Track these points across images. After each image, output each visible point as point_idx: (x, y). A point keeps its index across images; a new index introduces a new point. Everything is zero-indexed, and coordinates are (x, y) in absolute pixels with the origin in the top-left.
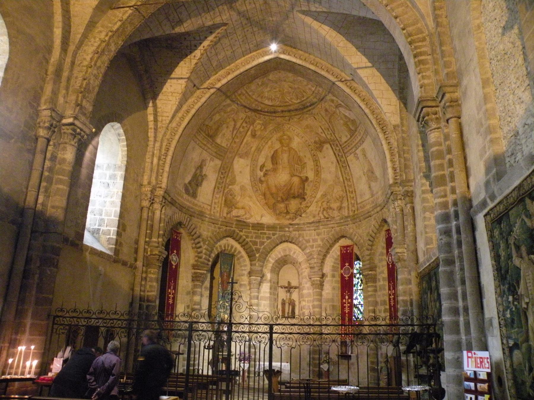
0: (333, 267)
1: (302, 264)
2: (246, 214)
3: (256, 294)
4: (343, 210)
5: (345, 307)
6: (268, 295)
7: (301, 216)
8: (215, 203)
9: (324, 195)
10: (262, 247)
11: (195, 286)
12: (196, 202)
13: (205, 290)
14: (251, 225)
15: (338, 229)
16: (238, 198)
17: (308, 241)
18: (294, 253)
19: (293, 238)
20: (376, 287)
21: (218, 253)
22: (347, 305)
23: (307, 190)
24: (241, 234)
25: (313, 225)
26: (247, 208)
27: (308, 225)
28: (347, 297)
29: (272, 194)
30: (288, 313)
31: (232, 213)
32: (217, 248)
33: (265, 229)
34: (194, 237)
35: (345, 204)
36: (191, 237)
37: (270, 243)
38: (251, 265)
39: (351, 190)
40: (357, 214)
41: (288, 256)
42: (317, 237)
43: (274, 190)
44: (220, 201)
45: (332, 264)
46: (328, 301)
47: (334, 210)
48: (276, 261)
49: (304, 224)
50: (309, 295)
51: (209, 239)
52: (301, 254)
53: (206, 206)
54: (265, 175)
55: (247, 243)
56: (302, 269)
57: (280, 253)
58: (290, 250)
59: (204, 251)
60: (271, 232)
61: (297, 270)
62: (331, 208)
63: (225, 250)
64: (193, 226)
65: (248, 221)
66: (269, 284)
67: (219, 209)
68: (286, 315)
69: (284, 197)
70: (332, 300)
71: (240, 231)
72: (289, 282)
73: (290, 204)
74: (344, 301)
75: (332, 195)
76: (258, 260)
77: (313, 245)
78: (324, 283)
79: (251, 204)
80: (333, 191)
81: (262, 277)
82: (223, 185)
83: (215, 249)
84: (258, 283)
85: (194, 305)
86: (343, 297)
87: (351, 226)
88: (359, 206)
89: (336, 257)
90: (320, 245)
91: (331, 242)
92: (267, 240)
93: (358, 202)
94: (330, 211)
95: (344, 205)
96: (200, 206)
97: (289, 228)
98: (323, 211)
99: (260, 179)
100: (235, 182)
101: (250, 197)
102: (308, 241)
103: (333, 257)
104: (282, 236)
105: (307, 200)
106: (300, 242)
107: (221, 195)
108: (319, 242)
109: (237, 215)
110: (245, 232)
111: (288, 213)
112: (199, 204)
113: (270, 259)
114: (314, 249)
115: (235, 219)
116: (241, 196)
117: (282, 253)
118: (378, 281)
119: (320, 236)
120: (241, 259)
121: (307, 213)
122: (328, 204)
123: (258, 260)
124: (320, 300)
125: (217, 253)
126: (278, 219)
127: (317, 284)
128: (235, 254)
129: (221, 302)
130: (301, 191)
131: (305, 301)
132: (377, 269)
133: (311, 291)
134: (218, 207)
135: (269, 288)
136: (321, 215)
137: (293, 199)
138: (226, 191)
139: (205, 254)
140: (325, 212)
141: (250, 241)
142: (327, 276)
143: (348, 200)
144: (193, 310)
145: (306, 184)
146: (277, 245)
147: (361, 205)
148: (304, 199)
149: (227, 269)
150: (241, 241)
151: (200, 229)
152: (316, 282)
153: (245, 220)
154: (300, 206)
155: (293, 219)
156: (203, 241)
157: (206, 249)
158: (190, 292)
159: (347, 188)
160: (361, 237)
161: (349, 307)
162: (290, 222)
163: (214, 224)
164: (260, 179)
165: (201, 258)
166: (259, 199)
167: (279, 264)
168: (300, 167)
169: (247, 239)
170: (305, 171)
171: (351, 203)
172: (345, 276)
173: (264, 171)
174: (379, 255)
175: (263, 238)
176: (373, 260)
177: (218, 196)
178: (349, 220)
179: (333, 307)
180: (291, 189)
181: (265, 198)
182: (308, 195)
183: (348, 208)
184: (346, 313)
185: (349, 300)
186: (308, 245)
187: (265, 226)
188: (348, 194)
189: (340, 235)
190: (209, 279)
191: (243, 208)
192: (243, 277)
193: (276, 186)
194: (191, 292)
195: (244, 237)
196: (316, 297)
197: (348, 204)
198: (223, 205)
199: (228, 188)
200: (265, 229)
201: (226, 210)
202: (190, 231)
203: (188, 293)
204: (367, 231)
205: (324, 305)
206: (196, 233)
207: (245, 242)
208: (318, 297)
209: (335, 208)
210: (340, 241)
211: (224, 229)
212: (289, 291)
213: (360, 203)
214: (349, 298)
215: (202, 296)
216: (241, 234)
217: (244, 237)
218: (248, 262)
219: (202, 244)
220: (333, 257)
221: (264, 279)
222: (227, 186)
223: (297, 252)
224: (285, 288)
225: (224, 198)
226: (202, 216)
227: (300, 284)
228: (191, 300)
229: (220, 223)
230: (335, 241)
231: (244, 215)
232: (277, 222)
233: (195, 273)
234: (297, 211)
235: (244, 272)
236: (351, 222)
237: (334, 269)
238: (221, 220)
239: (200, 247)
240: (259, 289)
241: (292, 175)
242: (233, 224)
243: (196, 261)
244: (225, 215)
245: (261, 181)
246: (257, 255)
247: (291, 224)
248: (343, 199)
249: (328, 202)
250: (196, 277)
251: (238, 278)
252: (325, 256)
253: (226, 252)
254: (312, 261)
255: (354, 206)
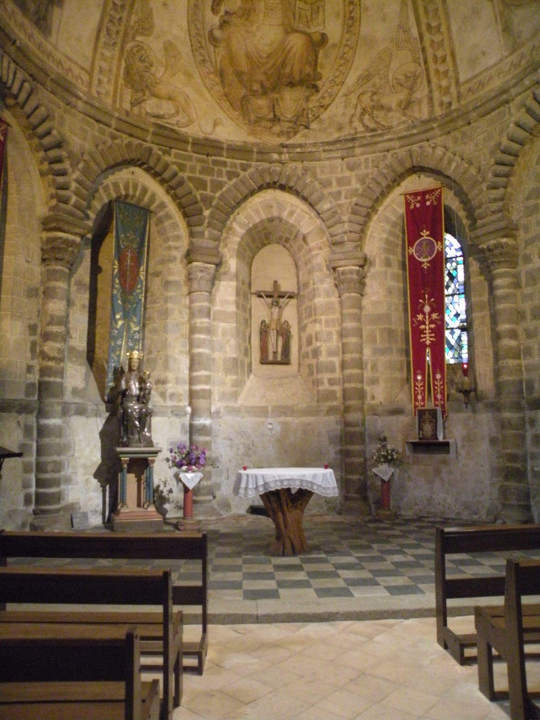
0: (387, 242)
1: (309, 240)
2: (177, 112)
3: (206, 304)
4: (416, 108)
5: (422, 332)
6: (232, 308)
7: (307, 127)
8: (101, 71)
9: (366, 78)
10: (218, 194)
11: (50, 275)
12: (49, 48)
13: (78, 290)
14: (190, 140)
15: (402, 153)
16: (159, 72)
17: (326, 184)
18: (292, 213)
19: (289, 178)
20: (517, 276)
21: (110, 202)
22: (427, 327)
23: (322, 67)
24: (167, 158)
25: (338, 146)
26: (181, 99)
27: (327, 148)
28: (427, 309)
29: (239, 74)
30: (275, 353)
31: (143, 104)
32: (106, 188)
33: (225, 154)
34: (46, 141)
35: (421, 92)
36: (36, 141)
37: (235, 186)
38: (192, 235)
39: (439, 54)
40: (456, 110)
41: (276, 222)
42: (348, 174)
43: (243, 65)
44: (114, 69)
45: (384, 236)
46: (377, 319)
47: (389, 110)
48: (249, 231)
49: (314, 145)
50: (329, 308)
51: (86, 157)
52: (307, 217)
53: (77, 71)
54: (224, 24)
55: (181, 183)
56: (310, 250)
57: (257, 212)
58: (281, 206)
59: (74, 186)
60: (238, 162)
61: (293, 256)
62: (382, 107)
63: (127, 196)
64: (42, 111)
65: (184, 130)
66: (234, 284)
67: (111, 89)
68: (271, 358)
69: (268, 84)
70: (386, 318)
71: (165, 152)
72: (275, 282)
73: (282, 99)
74: (420, 317)
75: (386, 76)
76: (210, 225)
77: (339, 193)
78: (367, 281)
79: (189, 91)
80: (388, 66)
81: (218, 265)
82: (122, 28)
83: (101, 191)
84: (209, 277)
85: (49, 324)
86: (416, 310)
87: (439, 140)
88: (463, 89)
89: (394, 218)
90: (357, 190)
91: (384, 183)
92: (230, 179)
93: (462, 79)
94: (380, 115)
95: (417, 95)
96: (60, 63)
97: (280, 153)
98: (362, 114)
99: (211, 32)
100: (151, 28)
101: (188, 75)
102: (326, 184)
103: (387, 220)
104: (261, 173)
105: (321, 92)
106: (306, 185)
107: (117, 54)
108: (355, 185)
109: (155, 111)
110: (177, 156)
111: (276, 119)
112: (58, 56)
113: (235, 225)
114: (343, 201)
115: (153, 120)
116: (166, 69)
117: (262, 212)
118: (520, 262)
119: (356, 172)
120: (167, 223)
121: (321, 122)
122: (375, 97)
123: (210, 225)
124: (358, 318)
125: (106, 200)
126: (253, 133)
127: (351, 280)
128: (153, 208)
129: (120, 323)
130: (308, 69)
131: (320, 322)
132: (521, 233)
133: (334, 299)
134: (109, 81)
135: (234, 292)
136: (357, 124)
137: (288, 89)
138: (128, 46)
139: (77, 193)
140: (366, 117)
141: (190, 178)
142: (372, 264)
143: (429, 82)
144: (47, 337)
145: (321, 53)
146: (252, 193)
147: (471, 84)
148: (316, 89)
149: (132, 241)
150: (166, 175)
151: (62, 124)
152: (349, 276)
153: (175, 128)
154: (304, 105)
155: (288, 135)
156: (69, 157)
157: (77, 181)
158: (37, 290)
159: (430, 52)
160: (470, 163)
161: (432, 330)
162: (282, 140)
163: (98, 121)
164: (211, 32)
165: (66, 202)
166: (207, 81)
167: (254, 241)
168: (308, 7)
169: (180, 174)
170: (320, 20)
171: (440, 87)
172: (421, 260)
173: (222, 13)
174: (528, 199)
175: (220, 174)
176: (508, 211)
177: (108, 54)
178: (435, 125)
179: (390, 333)
180: (283, 64)
181: (222, 82)
182: (324, 79)
183: (431, 99)
184: (425, 346)
185: (435, 316)
186: (326, 192)
187: (225, 146)
188: (432, 66)
189: (408, 165)
190: (86, 263)
191: (170, 98)
192: (171, 265)
193: (248, 56)
194: (42, 289)
195: (175, 167)
196: (351, 311)
197: (431, 91)
198: (121, 81)
199: (133, 39)
200: (225, 154)
201: (128, 95)
202: (34, 120)
203: (32, 293)
204: (492, 143)
205: (367, 329)
206: (48, 133)
207: (177, 179)
208: (355, 311)
209: (394, 106)
210: (404, 184)
211: (126, 142)
212: (278, 303)
213: (467, 82)
214: (432, 311)
215: (70, 303)
216: (167, 158)
217: (175, 167)
218: (183, 229)
219: (67, 165)
220: (387, 220)
221: (222, 270)
222: (131, 33)
223: (298, 210)
224: (268, 296)
225: (123, 65)
226: (67, 90)
227: (302, 285)
228: (40, 313)
229: (114, 123)
230: (394, 181)
231: (172, 116)
232: (251, 139)
233: (50, 240)
234: (298, 116)
235: (174, 253)
236: (437, 132)
237: (389, 246)
238: (116, 115)
239: (63, 173)
240: (210, 293)
241: (289, 30)
242: (148, 131)
243: (51, 209)
244: (127, 106)
245: (213, 40)
246: (207, 213)
247: (283, 146)
248: (415, 82)
249: (375, 93)
250: (53, 249)
251: (159, 268)
252: (368, 216)
253: (129, 200)
254: (338, 229)
255: (447, 91)
